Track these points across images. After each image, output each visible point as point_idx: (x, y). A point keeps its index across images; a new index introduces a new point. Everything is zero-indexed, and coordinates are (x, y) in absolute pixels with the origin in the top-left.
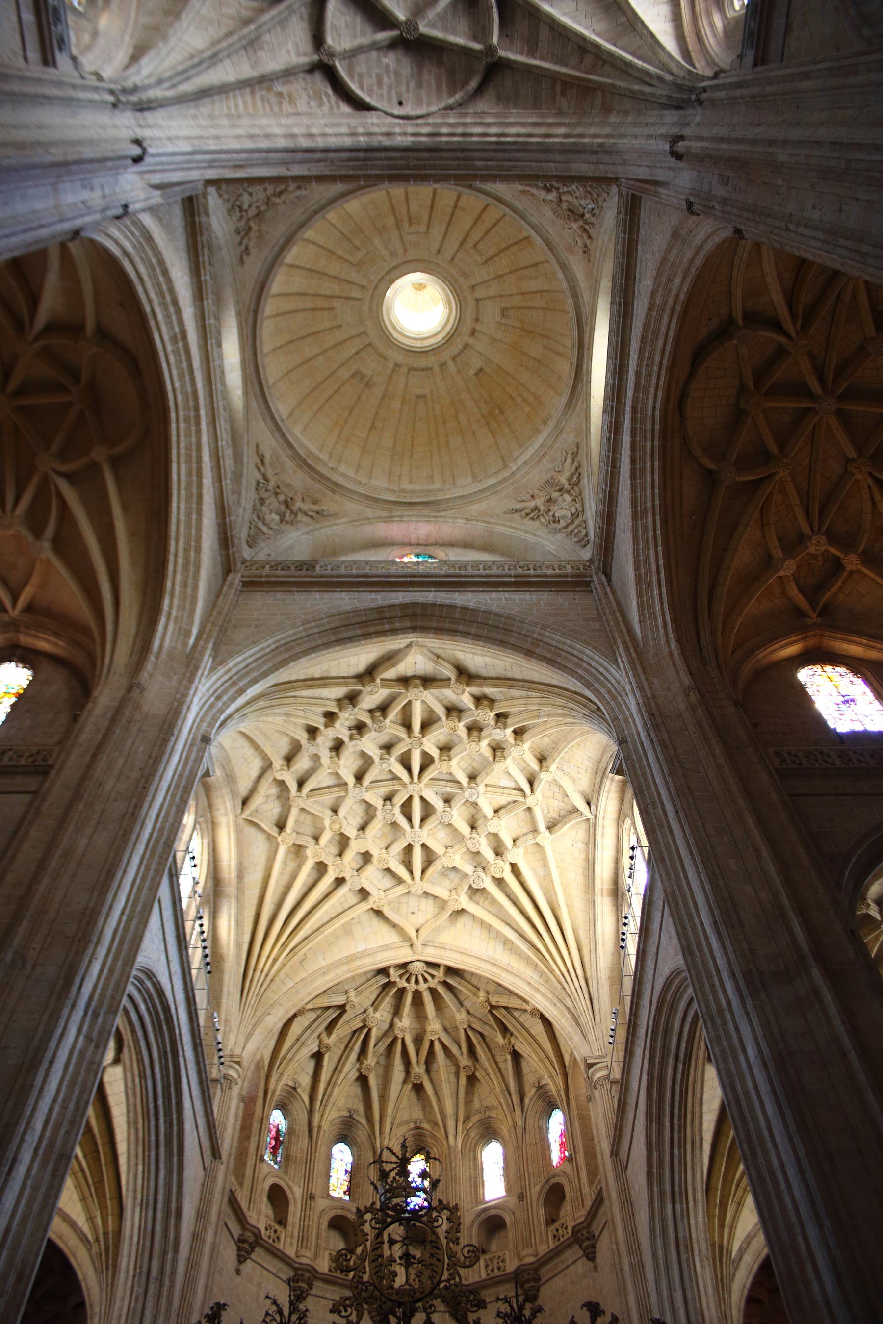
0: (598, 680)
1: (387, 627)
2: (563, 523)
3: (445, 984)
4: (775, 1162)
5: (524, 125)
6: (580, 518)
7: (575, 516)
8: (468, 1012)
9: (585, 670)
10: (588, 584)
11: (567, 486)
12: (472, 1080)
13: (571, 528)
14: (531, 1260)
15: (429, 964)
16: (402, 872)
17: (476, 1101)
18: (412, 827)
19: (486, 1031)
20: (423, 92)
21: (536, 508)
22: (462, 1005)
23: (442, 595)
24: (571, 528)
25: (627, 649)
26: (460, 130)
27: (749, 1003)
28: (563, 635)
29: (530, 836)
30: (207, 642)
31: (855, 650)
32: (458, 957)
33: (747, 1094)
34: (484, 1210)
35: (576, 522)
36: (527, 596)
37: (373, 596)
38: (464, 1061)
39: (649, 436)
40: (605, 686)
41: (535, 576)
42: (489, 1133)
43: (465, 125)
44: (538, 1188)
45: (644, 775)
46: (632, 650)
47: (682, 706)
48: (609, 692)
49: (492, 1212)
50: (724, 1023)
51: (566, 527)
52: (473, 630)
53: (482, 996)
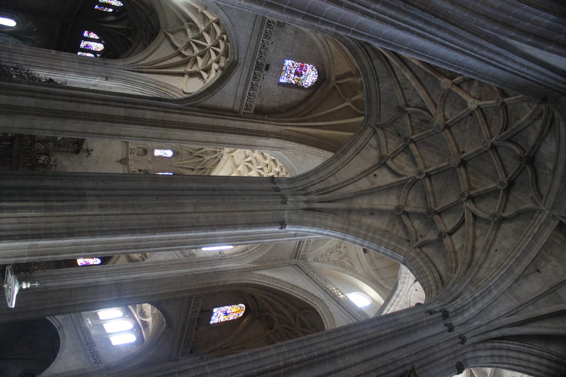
0: (250, 255)
2: (328, 254)
3: (217, 157)
4: (77, 278)
6: (327, 261)
7: (329, 260)
8: (208, 160)
9: (255, 253)
10: (295, 258)
11: (341, 260)
12: (191, 153)
13: (325, 256)
14: (130, 163)
15: (223, 155)
16: (248, 159)
17: (186, 152)
18: (258, 169)
19: (202, 163)
20: (417, 298)
21: (340, 247)
22: (212, 159)
24: (325, 256)
26: (395, 303)
27: (113, 282)
31: (245, 321)
32: (222, 165)
33: (95, 275)
34: (150, 150)
35: (325, 259)
38: (197, 153)
39: (312, 301)
40: (246, 257)
41: (302, 245)
42: (176, 154)
44: (151, 168)
45: (204, 264)
47: (221, 280)
48: (243, 258)
49: (149, 152)
50: (115, 273)
51: (326, 255)
53: (211, 167)
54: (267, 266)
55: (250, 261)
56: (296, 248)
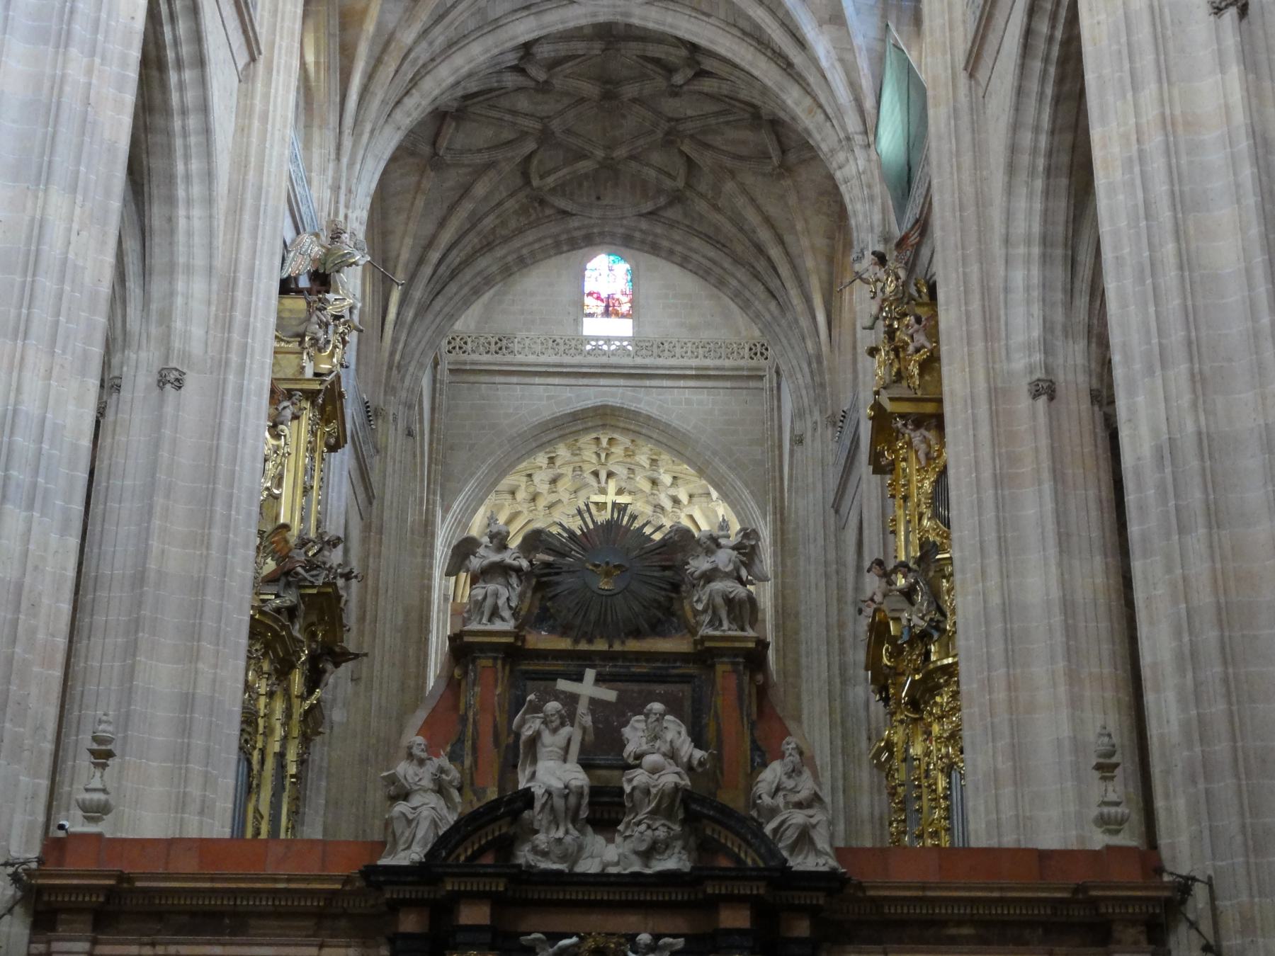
1: (581, 427)
5: (704, 256)
9: (742, 508)
18: (599, 482)
23: (629, 393)
25: (775, 513)
28: (730, 467)
29: (703, 499)
30: (435, 494)
36: (703, 396)
37: (568, 393)
43: (656, 235)
46: (778, 516)
52: (655, 436)
54: (774, 471)
55: (762, 523)
56: (728, 384)
